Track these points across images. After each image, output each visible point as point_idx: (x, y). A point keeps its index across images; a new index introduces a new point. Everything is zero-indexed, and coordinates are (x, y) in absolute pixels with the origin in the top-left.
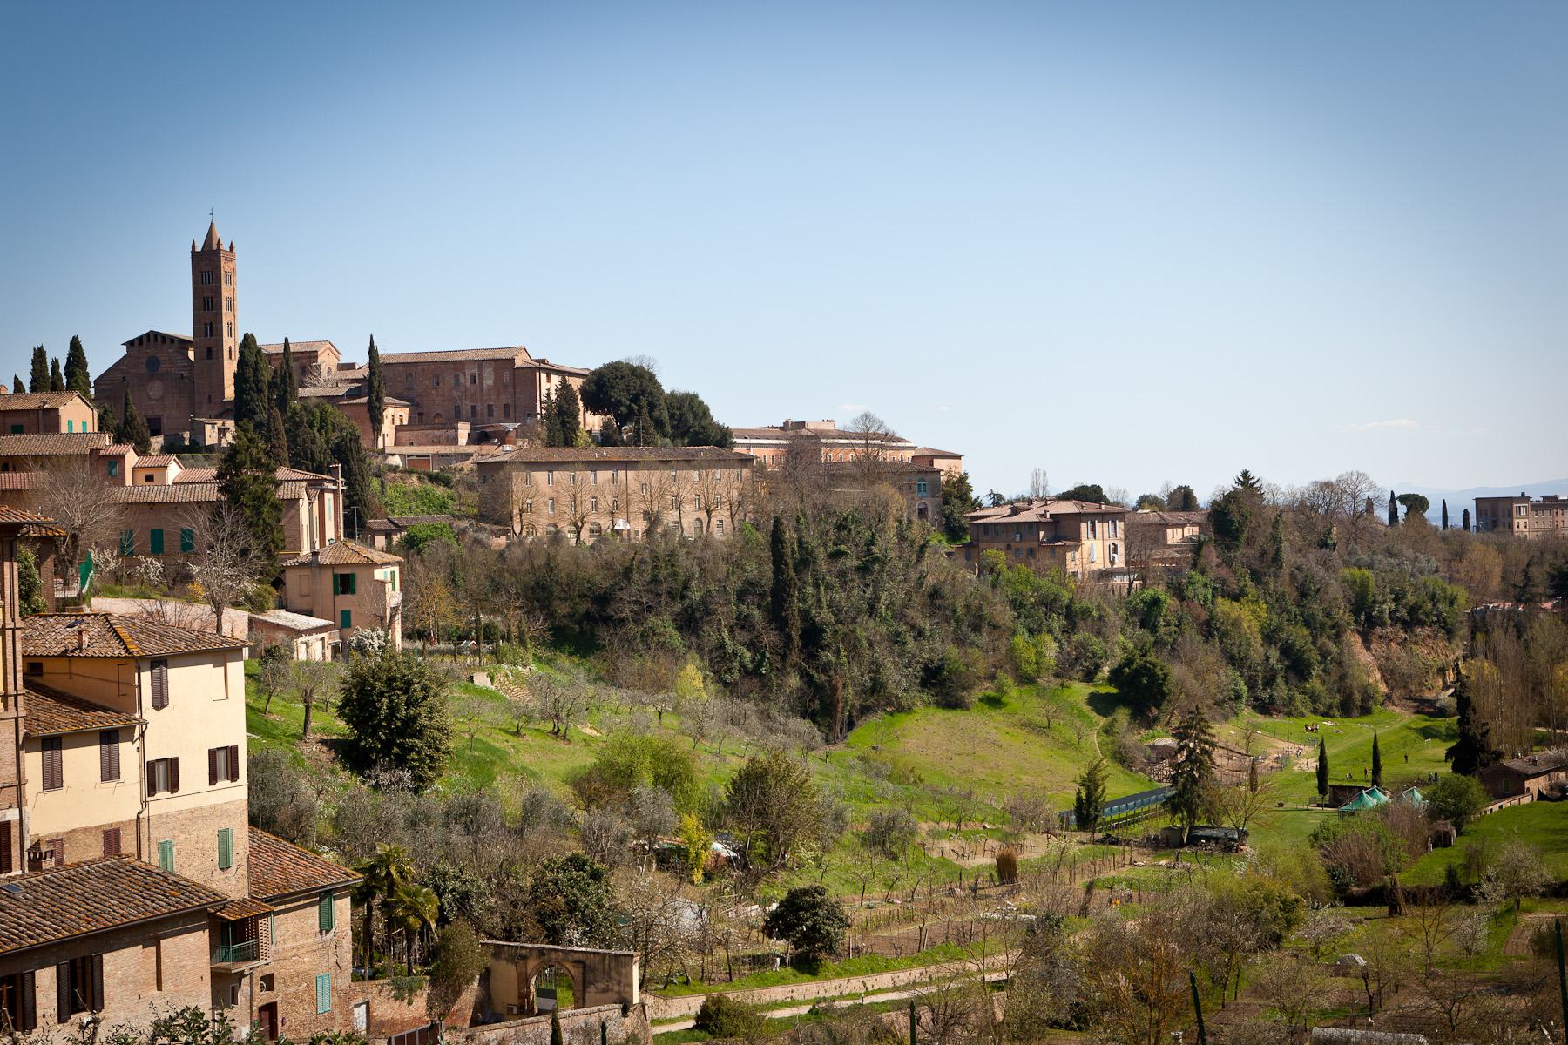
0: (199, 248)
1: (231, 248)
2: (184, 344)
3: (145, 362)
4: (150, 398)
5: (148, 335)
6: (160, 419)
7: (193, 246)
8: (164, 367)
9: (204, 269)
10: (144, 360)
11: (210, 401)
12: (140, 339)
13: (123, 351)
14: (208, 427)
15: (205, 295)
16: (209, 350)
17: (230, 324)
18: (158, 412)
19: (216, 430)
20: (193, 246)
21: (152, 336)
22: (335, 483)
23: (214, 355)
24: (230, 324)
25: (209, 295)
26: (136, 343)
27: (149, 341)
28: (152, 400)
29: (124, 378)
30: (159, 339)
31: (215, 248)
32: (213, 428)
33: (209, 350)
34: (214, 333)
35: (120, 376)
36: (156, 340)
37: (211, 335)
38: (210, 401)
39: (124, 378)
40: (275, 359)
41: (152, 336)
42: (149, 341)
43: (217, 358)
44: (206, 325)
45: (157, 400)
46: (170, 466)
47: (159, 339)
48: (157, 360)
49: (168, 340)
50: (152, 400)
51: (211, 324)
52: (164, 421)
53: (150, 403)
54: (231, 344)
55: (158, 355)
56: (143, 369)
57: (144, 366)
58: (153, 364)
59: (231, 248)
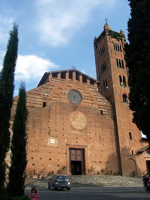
3: (67, 93)
5: (71, 72)
6: (83, 150)
11: (131, 138)
12: (63, 74)
18: (81, 143)
21: (74, 74)
26: (59, 75)
28: (74, 129)
29: (44, 104)
30: (81, 77)
35: (41, 101)
36: (77, 78)
38: (131, 138)
39: (44, 104)
41: (74, 74)
42: (71, 77)
47: (81, 77)
52: (88, 153)
53: (74, 132)
57: (66, 97)
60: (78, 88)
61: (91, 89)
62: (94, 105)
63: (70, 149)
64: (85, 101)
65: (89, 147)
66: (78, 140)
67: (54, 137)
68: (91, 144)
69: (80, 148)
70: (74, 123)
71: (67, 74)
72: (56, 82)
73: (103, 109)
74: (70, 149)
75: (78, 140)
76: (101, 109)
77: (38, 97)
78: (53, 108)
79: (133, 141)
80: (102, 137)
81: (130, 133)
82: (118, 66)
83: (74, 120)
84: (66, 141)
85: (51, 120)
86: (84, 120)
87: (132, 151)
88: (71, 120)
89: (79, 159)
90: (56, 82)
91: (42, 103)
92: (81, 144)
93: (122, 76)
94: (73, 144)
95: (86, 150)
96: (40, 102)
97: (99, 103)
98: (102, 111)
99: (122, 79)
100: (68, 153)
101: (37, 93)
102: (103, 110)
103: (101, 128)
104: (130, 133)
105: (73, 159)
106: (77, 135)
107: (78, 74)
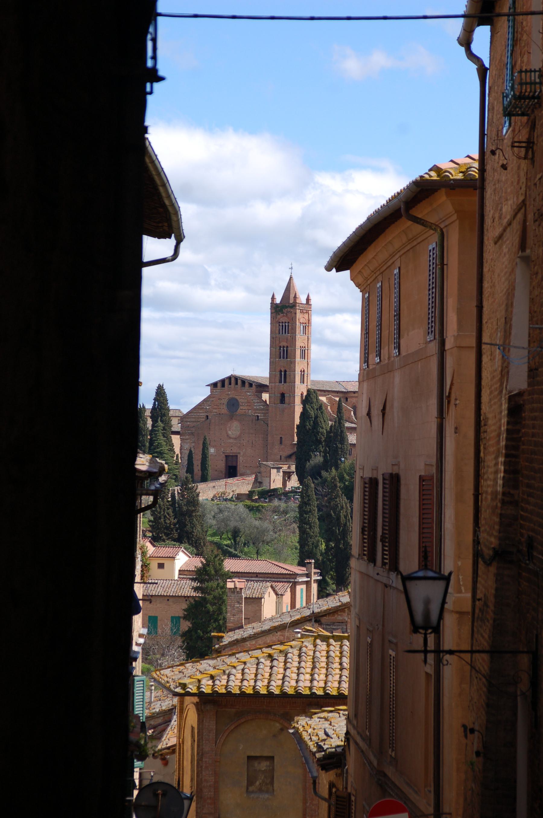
0: (278, 300)
1: (308, 300)
2: (261, 387)
3: (226, 403)
4: (229, 437)
5: (230, 378)
6: (237, 456)
7: (273, 298)
8: (242, 409)
9: (281, 320)
10: (225, 401)
11: (281, 443)
12: (223, 381)
13: (207, 392)
14: (274, 471)
15: (282, 344)
16: (283, 395)
17: (303, 371)
18: (235, 450)
19: (281, 474)
20: (273, 298)
22: (308, 575)
23: (287, 399)
24: (303, 371)
25: (285, 344)
26: (219, 385)
27: (230, 384)
28: (230, 438)
29: (207, 416)
31: (291, 301)
32: (278, 472)
33: (283, 395)
34: (288, 380)
35: (204, 415)
36: (237, 384)
37: (285, 382)
38: (281, 443)
40: (352, 397)
41: (233, 380)
42: (230, 384)
43: (289, 404)
44: (281, 371)
45: (235, 439)
46: (177, 557)
48: (237, 400)
49: (247, 384)
50: (230, 438)
51: (285, 371)
52: (241, 459)
54: (300, 389)
55: (236, 397)
56: (224, 410)
57: (225, 407)
58: (233, 404)
59: (308, 300)
60: (237, 394)
61: (248, 394)
62: (250, 411)
63: (226, 456)
64: (241, 407)
65: (242, 454)
66: (232, 448)
67: (213, 447)
68: (244, 451)
69: (234, 455)
70: (230, 433)
71: (227, 382)
72: (216, 393)
73: (259, 413)
74: (226, 456)
75: (232, 448)
76: (256, 414)
77: (201, 411)
78: (213, 421)
79: (283, 446)
80: (254, 443)
81: (281, 438)
82: (280, 358)
83: (230, 430)
84: (222, 449)
85: (211, 432)
86: (239, 429)
87: (281, 456)
88: (228, 429)
89: (234, 464)
90: (216, 393)
91: (205, 417)
92: (235, 451)
93: (283, 370)
94: (228, 451)
95: (238, 457)
96: (203, 416)
97: (255, 407)
98: (258, 416)
99: (283, 373)
100: (224, 459)
101: (201, 407)
102: (259, 415)
103: (254, 435)
104: (281, 438)
105: (230, 465)
106: (232, 443)
107: (236, 379)
